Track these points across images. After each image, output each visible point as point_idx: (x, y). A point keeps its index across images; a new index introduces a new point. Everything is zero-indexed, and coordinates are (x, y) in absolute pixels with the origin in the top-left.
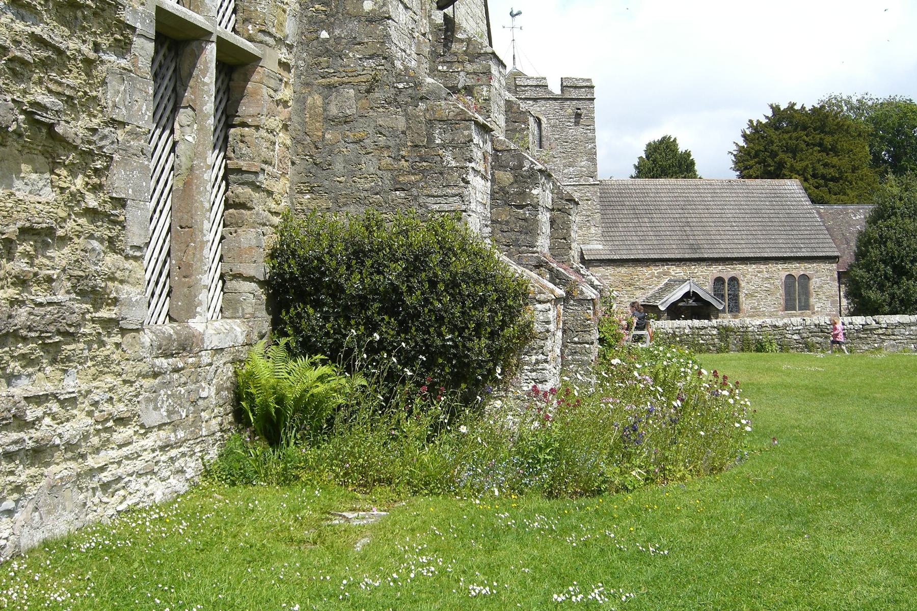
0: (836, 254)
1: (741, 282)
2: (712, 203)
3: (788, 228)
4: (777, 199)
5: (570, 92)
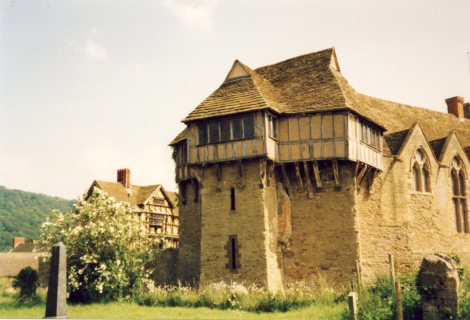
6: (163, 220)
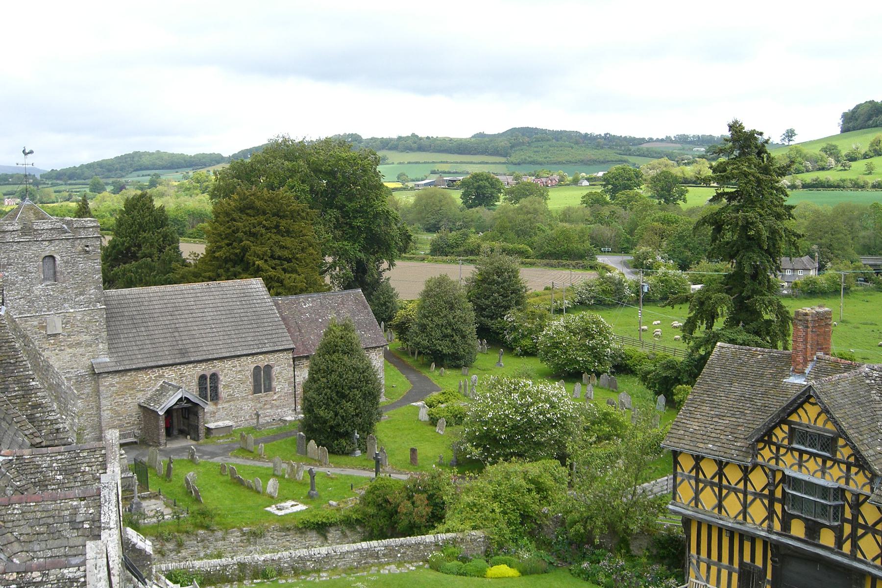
0: (292, 346)
1: (220, 376)
2: (194, 307)
3: (255, 326)
4: (246, 298)
5: (80, 232)
6: (843, 506)
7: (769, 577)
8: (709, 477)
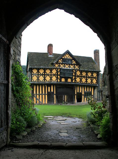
6: (73, 73)
7: (55, 93)
8: (41, 73)
